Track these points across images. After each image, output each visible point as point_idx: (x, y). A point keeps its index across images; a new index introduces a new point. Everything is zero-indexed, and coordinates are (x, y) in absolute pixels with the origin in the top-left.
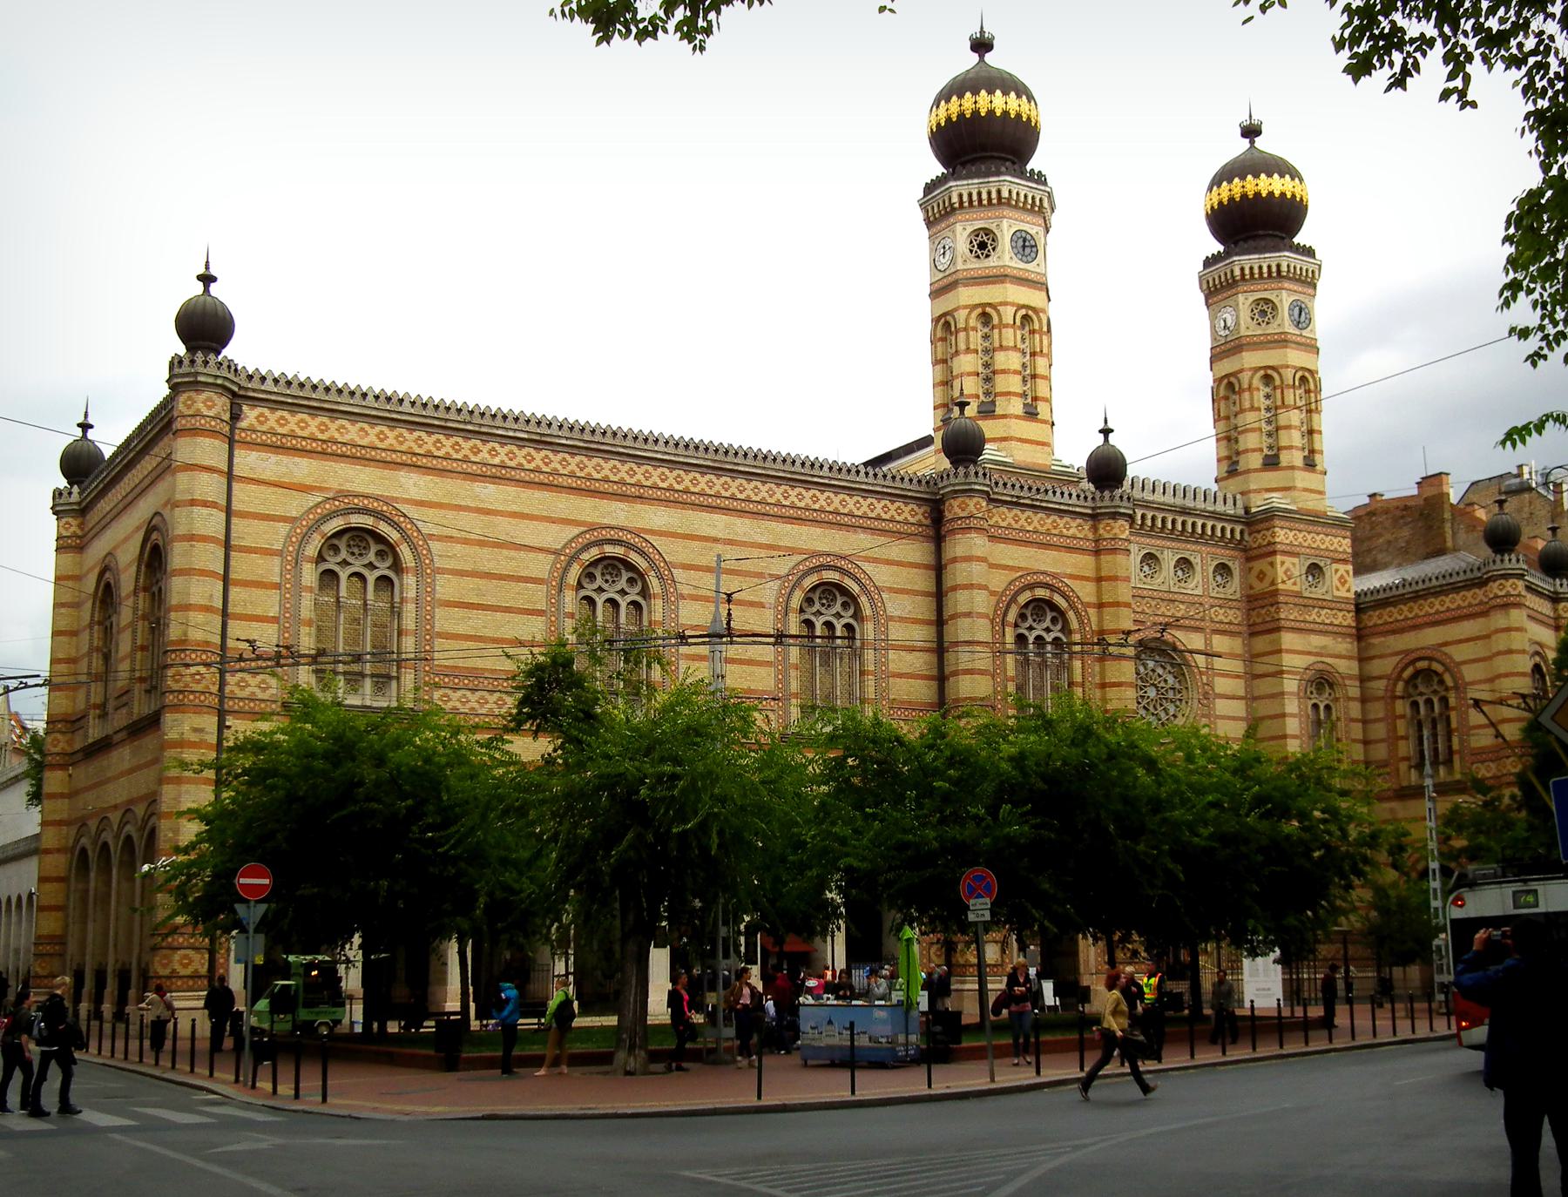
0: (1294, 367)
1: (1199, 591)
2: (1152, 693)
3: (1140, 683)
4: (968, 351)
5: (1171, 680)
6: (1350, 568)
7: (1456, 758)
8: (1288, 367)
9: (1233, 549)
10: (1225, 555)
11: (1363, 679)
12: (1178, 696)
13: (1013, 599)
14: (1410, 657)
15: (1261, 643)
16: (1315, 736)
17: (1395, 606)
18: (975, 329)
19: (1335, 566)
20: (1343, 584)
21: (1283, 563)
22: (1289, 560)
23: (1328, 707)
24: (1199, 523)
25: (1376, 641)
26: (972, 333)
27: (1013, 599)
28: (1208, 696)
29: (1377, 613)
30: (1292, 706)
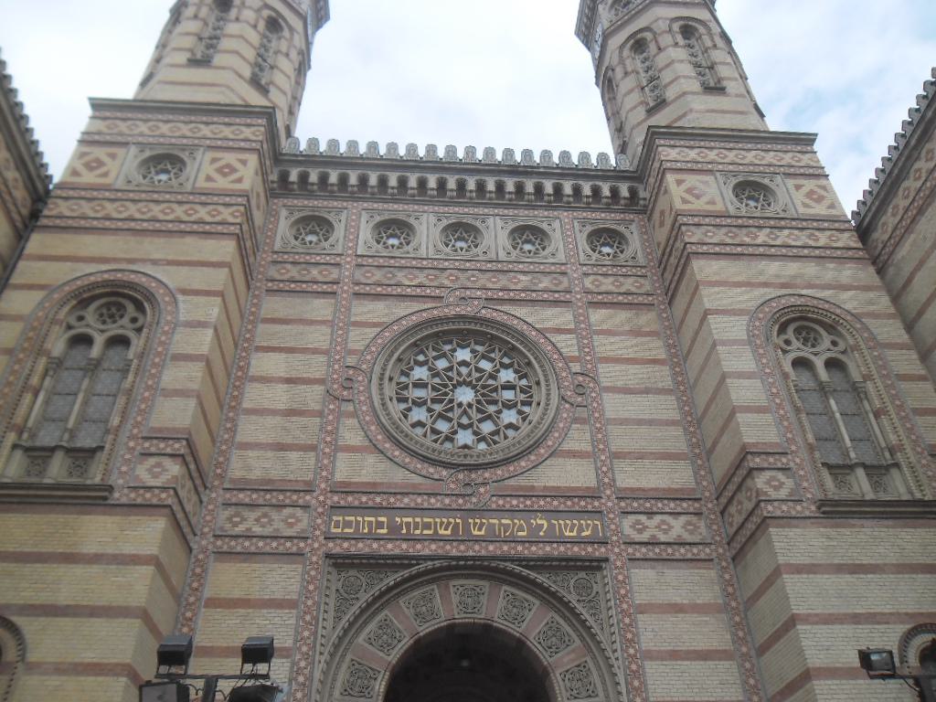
0: (666, 19)
1: (561, 257)
2: (465, 395)
3: (437, 380)
5: (507, 376)
10: (607, 219)
12: (522, 397)
15: (681, 301)
17: (906, 178)
19: (791, 183)
22: (692, 180)
23: (832, 364)
24: (548, 187)
25: (902, 252)
28: (584, 386)
29: (890, 210)
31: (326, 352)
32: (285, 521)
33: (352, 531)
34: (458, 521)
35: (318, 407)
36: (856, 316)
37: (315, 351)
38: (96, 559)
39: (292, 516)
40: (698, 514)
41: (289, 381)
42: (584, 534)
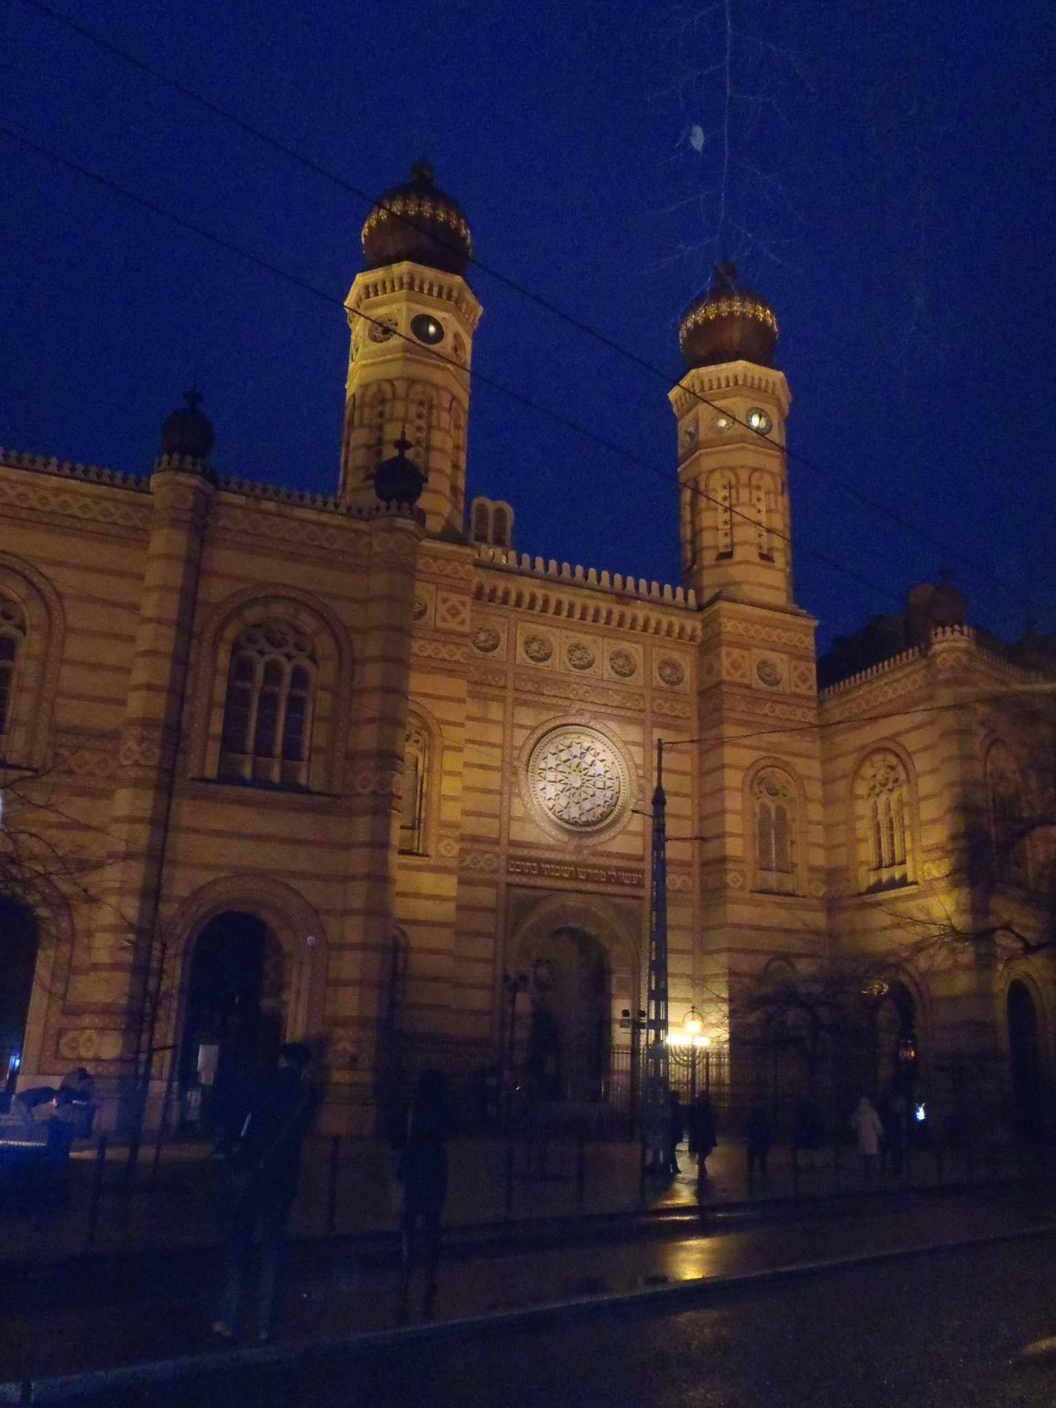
4: (362, 425)
6: (813, 666)
7: (909, 859)
8: (742, 467)
9: (683, 644)
11: (826, 782)
13: (237, 612)
14: (868, 753)
16: (763, 836)
18: (372, 407)
20: (804, 681)
21: (729, 654)
22: (736, 653)
25: (838, 739)
26: (367, 411)
27: (237, 612)
30: (734, 802)
31: (501, 747)
32: (486, 862)
33: (518, 870)
34: (573, 869)
35: (498, 788)
36: (801, 777)
37: (494, 745)
38: (429, 897)
39: (488, 860)
40: (689, 874)
41: (482, 767)
42: (633, 882)
